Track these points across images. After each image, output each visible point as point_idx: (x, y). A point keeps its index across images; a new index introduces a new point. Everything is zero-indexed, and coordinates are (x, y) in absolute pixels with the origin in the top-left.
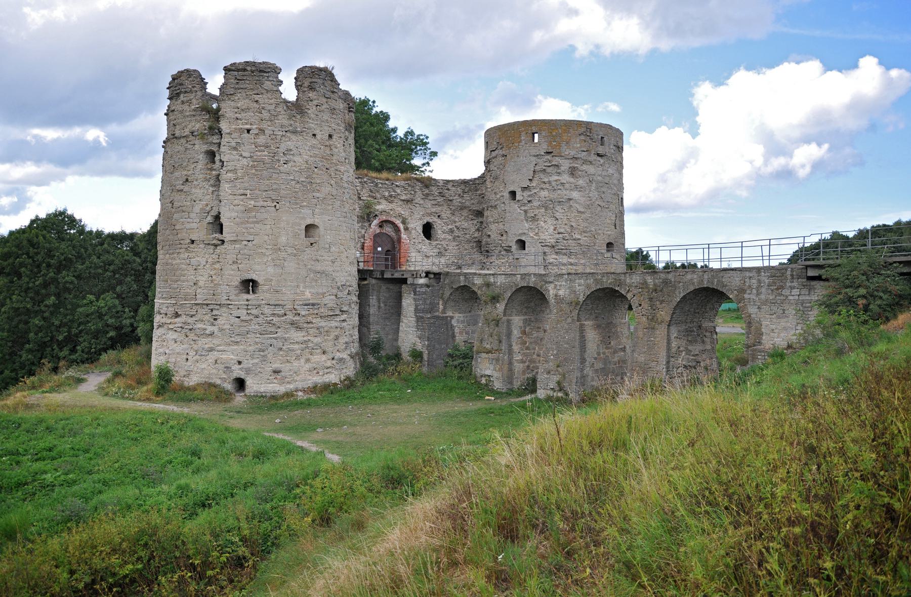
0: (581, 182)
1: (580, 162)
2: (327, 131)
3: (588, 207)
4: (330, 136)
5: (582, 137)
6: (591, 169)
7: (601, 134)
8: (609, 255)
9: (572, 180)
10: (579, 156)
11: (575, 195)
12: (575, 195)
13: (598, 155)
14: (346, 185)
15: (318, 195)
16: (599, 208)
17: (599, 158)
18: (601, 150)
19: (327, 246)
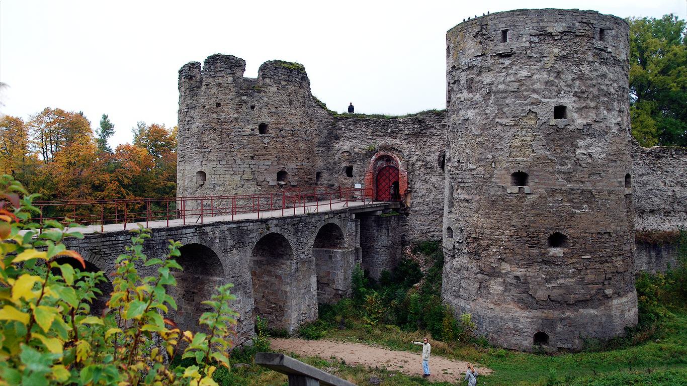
0: (478, 97)
1: (476, 71)
2: (213, 102)
3: (484, 128)
4: (218, 105)
5: (479, 38)
6: (487, 78)
7: (502, 27)
8: (516, 189)
9: (471, 95)
10: (474, 63)
11: (471, 114)
12: (471, 114)
13: (501, 56)
14: (235, 139)
15: (205, 150)
16: (499, 128)
17: (501, 60)
18: (502, 48)
19: (212, 187)
